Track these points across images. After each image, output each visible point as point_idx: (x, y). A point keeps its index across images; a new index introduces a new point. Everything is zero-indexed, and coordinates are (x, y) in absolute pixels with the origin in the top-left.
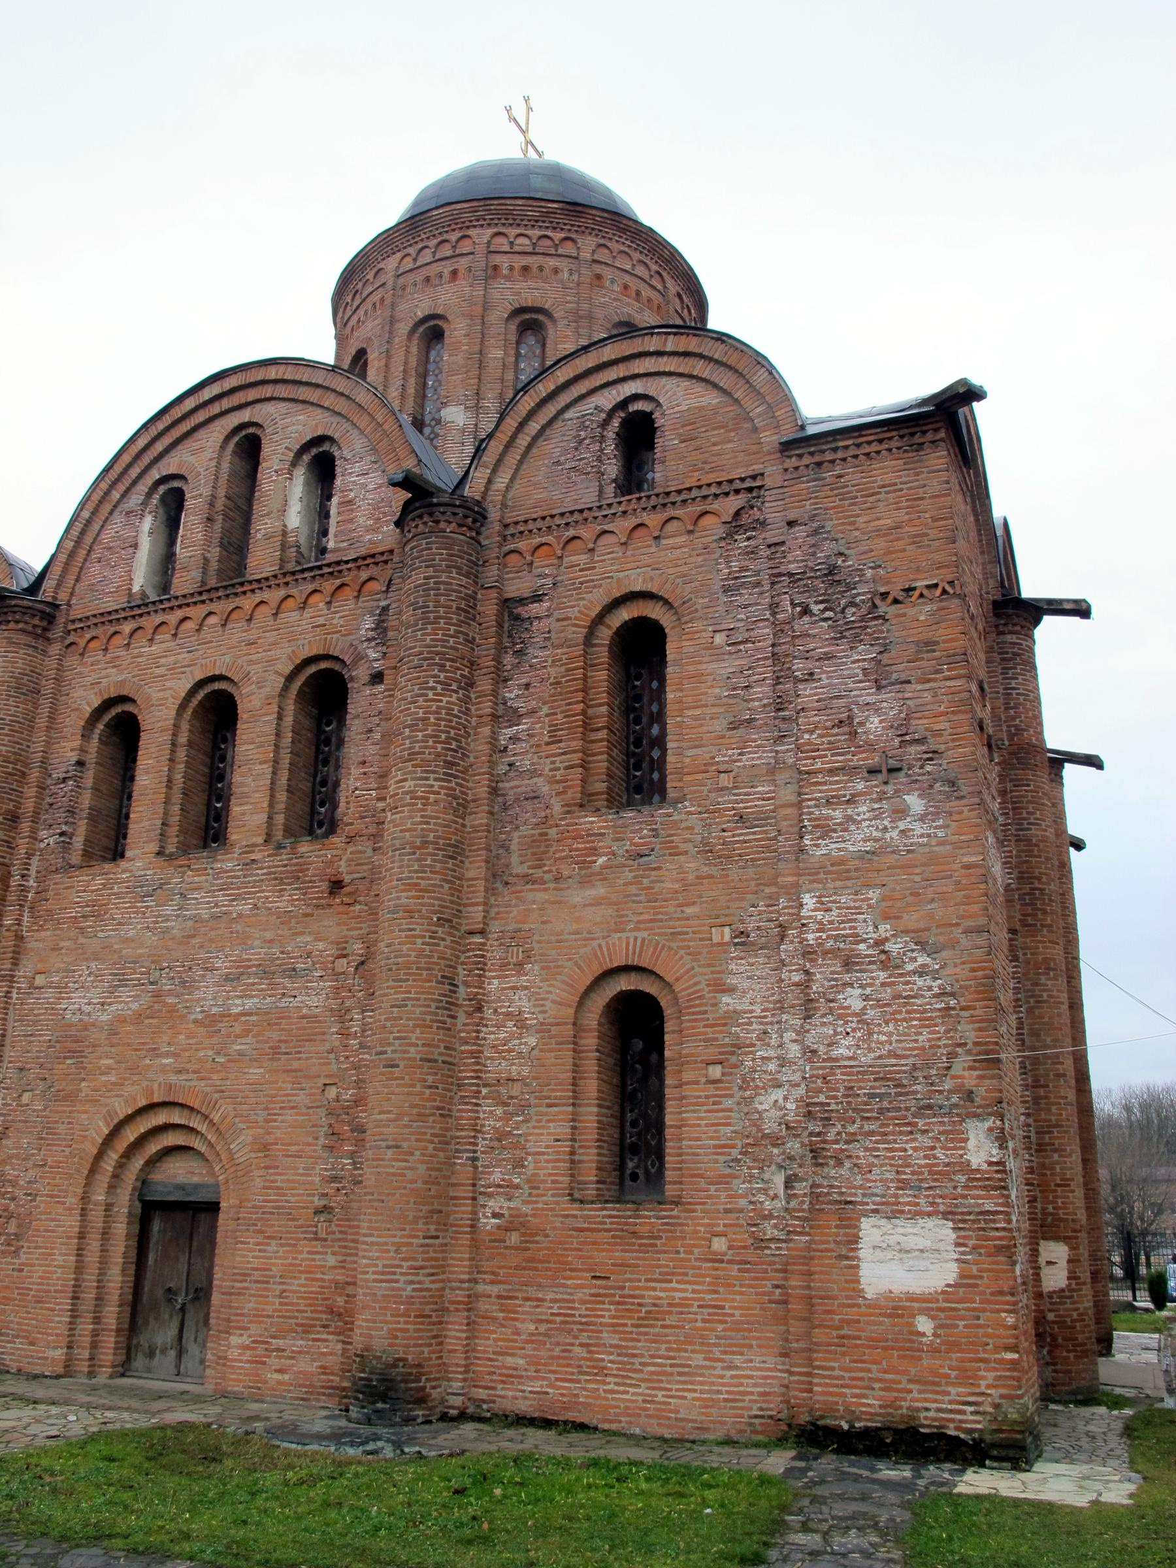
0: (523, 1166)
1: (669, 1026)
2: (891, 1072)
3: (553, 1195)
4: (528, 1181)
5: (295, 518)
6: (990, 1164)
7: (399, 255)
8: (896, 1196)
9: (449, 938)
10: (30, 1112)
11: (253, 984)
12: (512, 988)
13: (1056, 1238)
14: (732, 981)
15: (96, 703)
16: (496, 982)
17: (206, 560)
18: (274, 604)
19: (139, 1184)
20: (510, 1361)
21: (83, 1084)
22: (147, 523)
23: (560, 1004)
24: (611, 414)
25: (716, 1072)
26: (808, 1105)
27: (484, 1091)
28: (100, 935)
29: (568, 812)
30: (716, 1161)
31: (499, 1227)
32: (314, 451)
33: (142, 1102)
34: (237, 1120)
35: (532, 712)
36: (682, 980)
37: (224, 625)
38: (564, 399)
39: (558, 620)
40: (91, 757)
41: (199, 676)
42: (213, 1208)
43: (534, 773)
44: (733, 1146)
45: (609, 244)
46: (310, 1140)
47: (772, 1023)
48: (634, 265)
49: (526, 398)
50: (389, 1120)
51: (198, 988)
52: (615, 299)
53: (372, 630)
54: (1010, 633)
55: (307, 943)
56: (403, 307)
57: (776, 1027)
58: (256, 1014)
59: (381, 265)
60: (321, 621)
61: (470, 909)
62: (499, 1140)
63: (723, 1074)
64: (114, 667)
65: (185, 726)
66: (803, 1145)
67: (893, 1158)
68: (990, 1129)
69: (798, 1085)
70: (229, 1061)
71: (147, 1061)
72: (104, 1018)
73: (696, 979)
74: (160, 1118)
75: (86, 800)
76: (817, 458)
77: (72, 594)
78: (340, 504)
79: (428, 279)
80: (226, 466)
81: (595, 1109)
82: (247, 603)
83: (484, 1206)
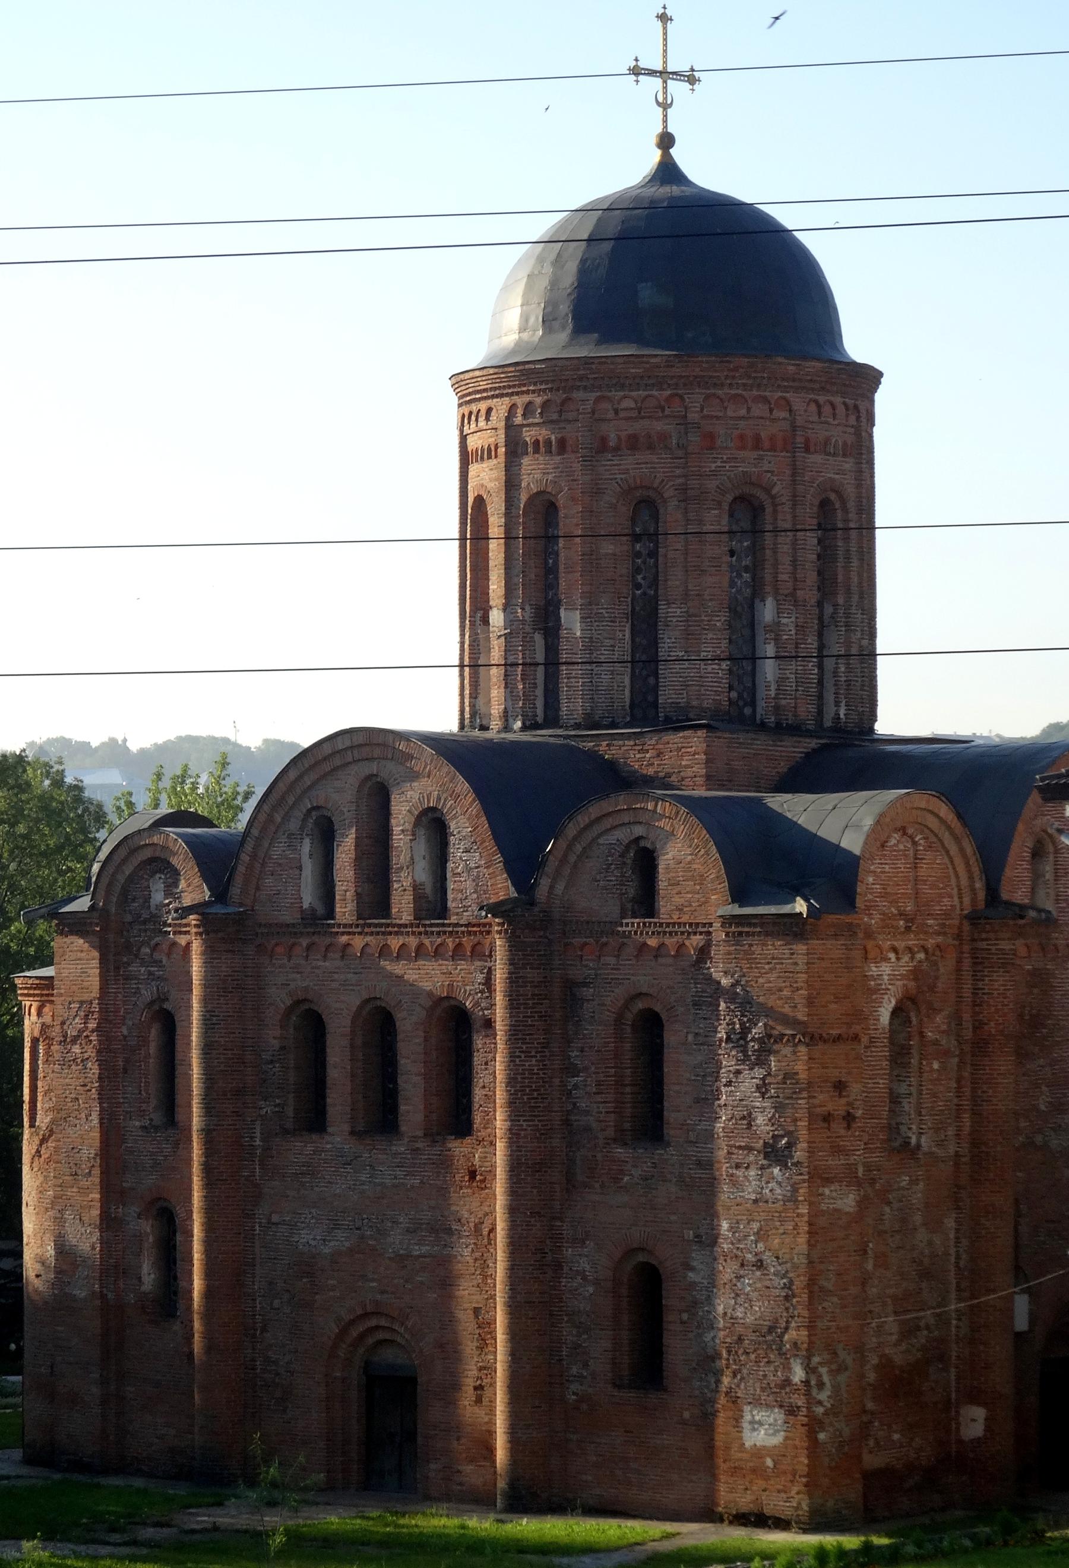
0: (588, 1365)
6: (802, 1382)
8: (760, 1395)
9: (538, 1224)
10: (281, 1314)
11: (426, 1236)
12: (580, 1255)
13: (979, 1404)
14: (695, 1264)
15: (289, 1002)
16: (570, 1250)
19: (363, 1364)
20: (584, 1477)
21: (317, 1297)
22: (306, 846)
24: (628, 847)
25: (685, 1316)
28: (315, 1188)
29: (608, 1144)
31: (576, 1401)
33: (360, 1312)
35: (586, 1069)
38: (596, 830)
39: (599, 1005)
41: (365, 996)
42: (412, 1381)
43: (587, 1113)
48: (749, 410)
49: (570, 825)
51: (389, 1236)
64: (298, 973)
72: (327, 1251)
74: (373, 1322)
76: (740, 929)
83: (568, 1388)
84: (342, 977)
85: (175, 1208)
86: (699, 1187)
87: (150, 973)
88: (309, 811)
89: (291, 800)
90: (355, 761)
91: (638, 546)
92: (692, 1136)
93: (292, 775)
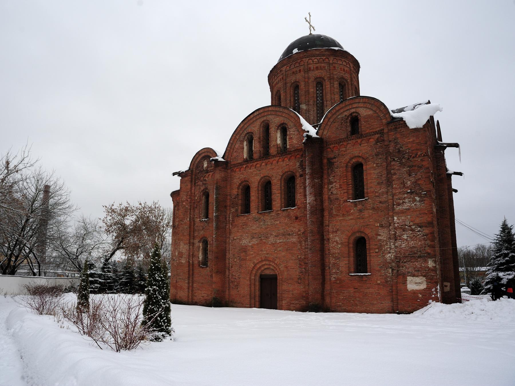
1: (367, 242)
2: (413, 250)
3: (346, 274)
4: (340, 272)
5: (279, 141)
6: (433, 267)
7: (286, 66)
8: (414, 273)
12: (335, 236)
16: (331, 235)
17: (260, 151)
18: (277, 161)
21: (247, 257)
22: (245, 143)
23: (345, 239)
25: (377, 250)
26: (396, 256)
27: (330, 255)
28: (247, 229)
30: (378, 267)
32: (281, 126)
34: (280, 262)
36: (369, 234)
37: (266, 165)
40: (240, 193)
41: (262, 176)
44: (381, 264)
45: (336, 58)
46: (296, 266)
47: (388, 241)
48: (342, 62)
50: (313, 261)
51: (270, 238)
52: (339, 72)
53: (299, 165)
54: (438, 152)
55: (292, 229)
56: (288, 80)
57: (389, 242)
58: (283, 243)
59: (281, 69)
60: (288, 164)
61: (325, 221)
62: (334, 264)
63: (379, 251)
64: (243, 174)
65: (260, 186)
66: (395, 264)
67: (413, 266)
68: (433, 260)
69: (394, 253)
70: (277, 252)
71: (260, 252)
72: (250, 245)
73: (372, 233)
75: (240, 202)
77: (231, 159)
78: (289, 138)
79: (293, 72)
80: (261, 130)
81: (353, 258)
82: (271, 160)
83: (332, 276)
84: (255, 173)
85: (208, 239)
86: (381, 209)
87: (203, 183)
88: (246, 134)
89: (241, 132)
90: (260, 118)
91: (318, 92)
92: (377, 194)
93: (242, 125)
